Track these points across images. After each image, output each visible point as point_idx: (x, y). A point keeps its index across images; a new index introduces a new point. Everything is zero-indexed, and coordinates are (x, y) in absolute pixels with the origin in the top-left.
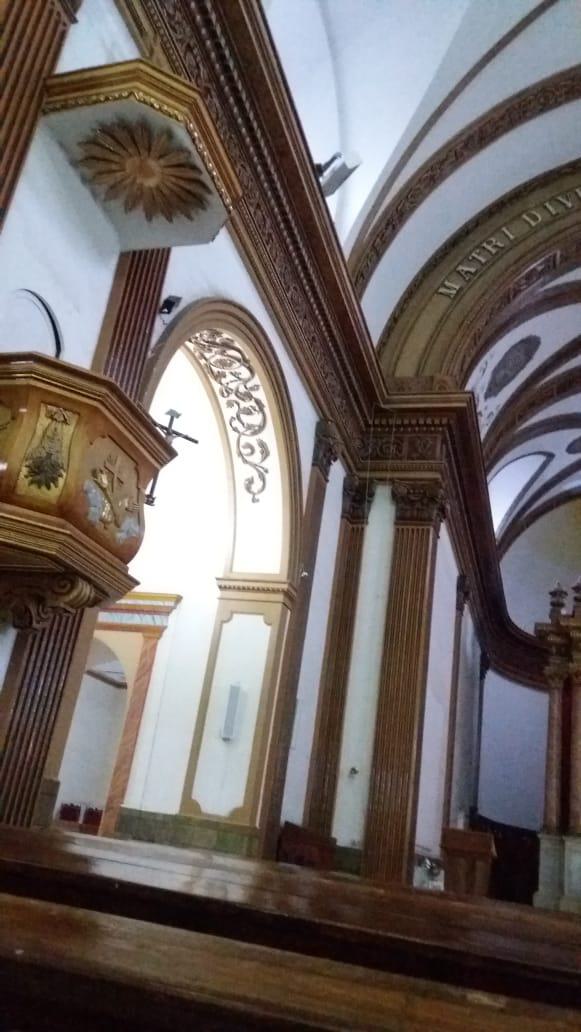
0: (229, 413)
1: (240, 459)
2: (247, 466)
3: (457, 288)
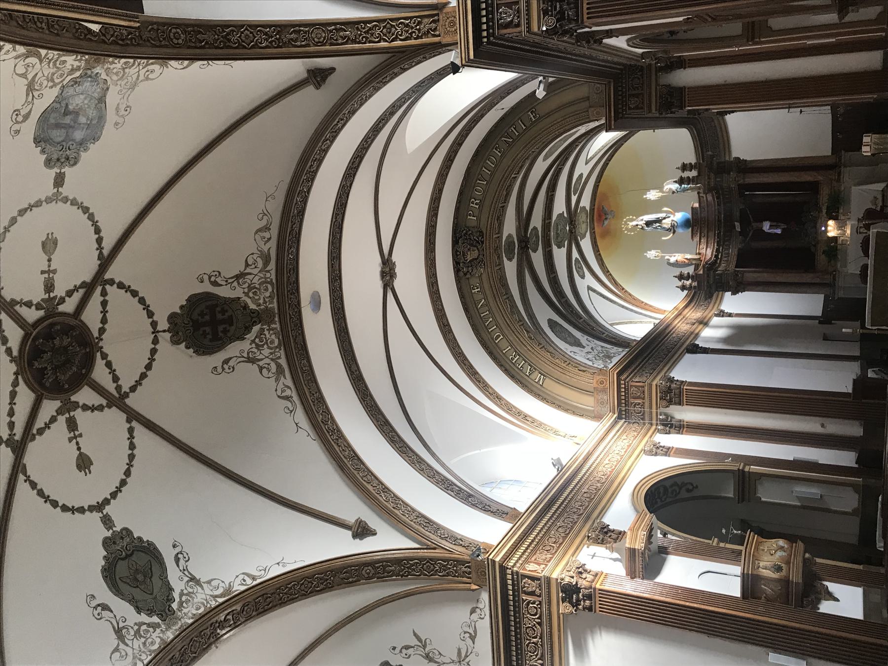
3: (540, 375)
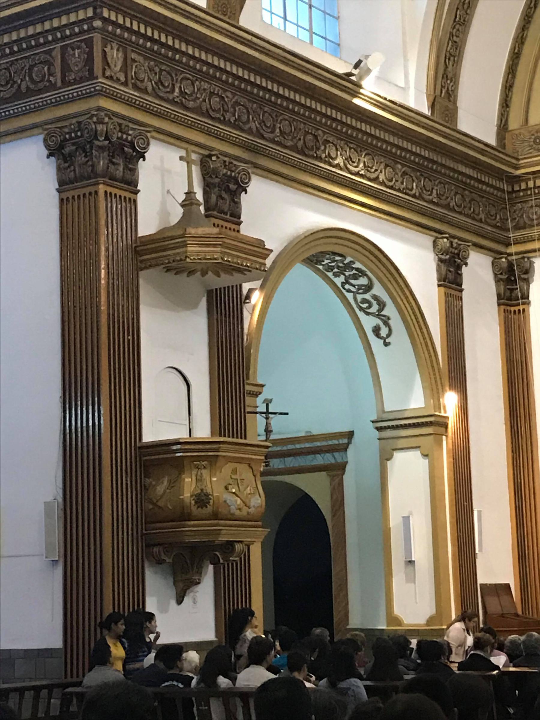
0: (339, 281)
1: (362, 313)
2: (371, 317)
